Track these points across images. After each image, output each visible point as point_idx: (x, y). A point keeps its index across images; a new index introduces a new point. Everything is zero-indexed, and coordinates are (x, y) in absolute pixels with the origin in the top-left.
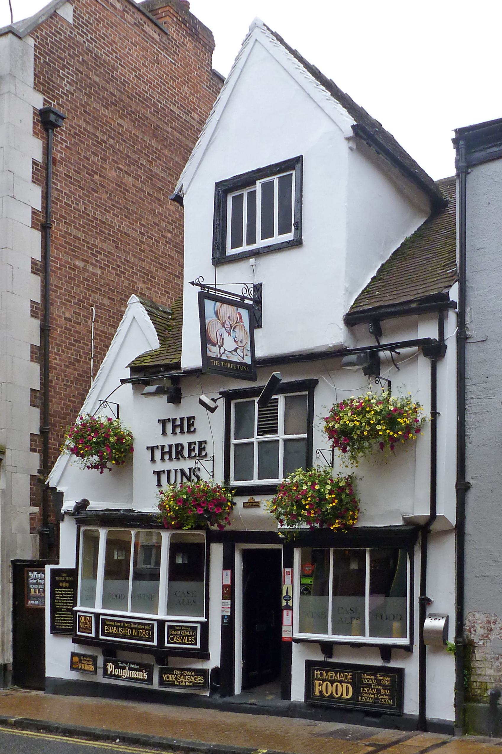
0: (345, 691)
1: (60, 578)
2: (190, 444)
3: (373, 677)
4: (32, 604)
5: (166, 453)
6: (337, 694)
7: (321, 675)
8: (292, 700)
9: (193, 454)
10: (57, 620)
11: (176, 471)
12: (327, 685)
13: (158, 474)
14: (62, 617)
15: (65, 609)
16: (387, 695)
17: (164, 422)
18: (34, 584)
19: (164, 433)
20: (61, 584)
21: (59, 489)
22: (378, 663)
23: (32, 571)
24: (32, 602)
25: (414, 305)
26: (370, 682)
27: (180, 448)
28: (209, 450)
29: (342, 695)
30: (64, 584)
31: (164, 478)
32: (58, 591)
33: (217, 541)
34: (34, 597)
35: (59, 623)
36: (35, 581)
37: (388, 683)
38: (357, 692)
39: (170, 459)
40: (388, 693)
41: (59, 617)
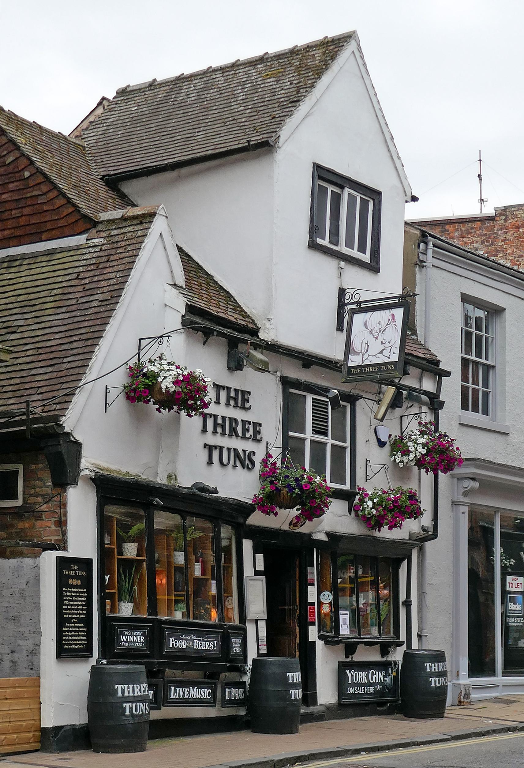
1: (69, 573)
9: (248, 435)
10: (66, 636)
11: (229, 449)
13: (210, 448)
14: (72, 631)
15: (75, 618)
20: (70, 581)
21: (78, 436)
30: (75, 582)
32: (66, 592)
35: (69, 640)
41: (68, 631)
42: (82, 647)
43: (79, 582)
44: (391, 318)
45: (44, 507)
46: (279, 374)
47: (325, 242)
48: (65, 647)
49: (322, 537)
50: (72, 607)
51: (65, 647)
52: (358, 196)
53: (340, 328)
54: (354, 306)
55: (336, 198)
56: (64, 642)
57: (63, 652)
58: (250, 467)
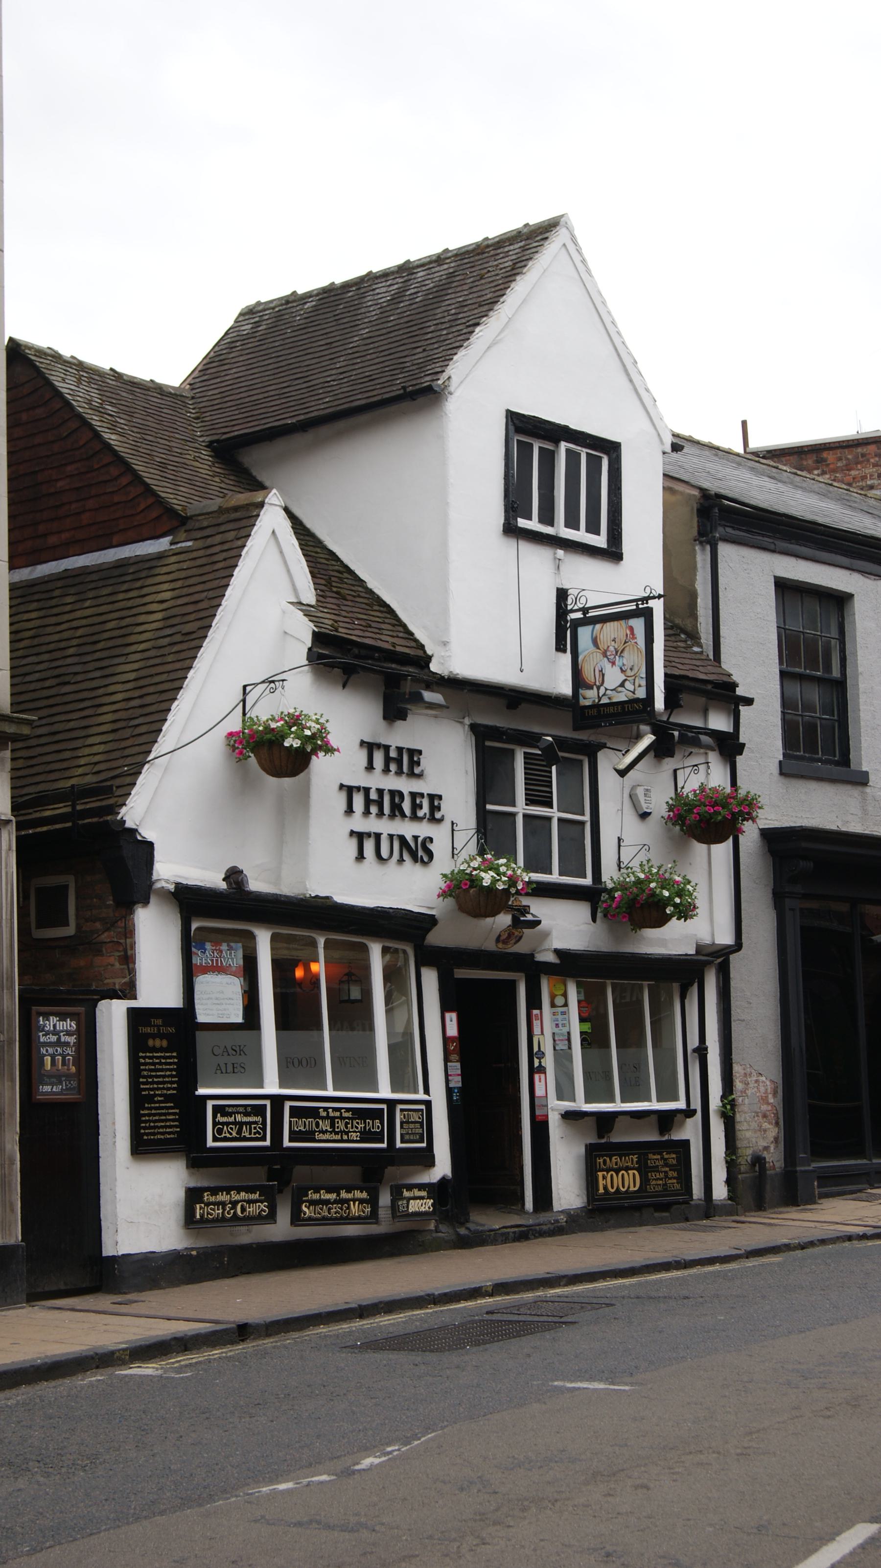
0: (630, 1181)
1: (148, 1030)
2: (414, 795)
3: (659, 1157)
4: (47, 1093)
5: (374, 802)
6: (623, 1187)
7: (605, 1162)
8: (555, 1209)
9: (420, 814)
10: (145, 1122)
11: (391, 836)
12: (612, 1176)
13: (360, 837)
14: (155, 1115)
15: (160, 1095)
16: (674, 1178)
17: (370, 747)
18: (50, 1044)
19: (370, 767)
20: (151, 1043)
22: (653, 1137)
23: (46, 1016)
24: (47, 1088)
25: (709, 687)
26: (657, 1163)
27: (397, 800)
28: (447, 809)
29: (629, 1187)
30: (158, 1043)
31: (369, 847)
32: (144, 1058)
33: (429, 964)
34: (50, 1076)
35: (150, 1128)
36: (53, 1038)
37: (675, 1162)
38: (645, 1181)
39: (381, 814)
40: (675, 1175)
41: (149, 1115)
42: (172, 1136)
43: (165, 1043)
44: (628, 632)
45: (104, 937)
46: (467, 721)
47: (533, 524)
48: (145, 1137)
49: (551, 958)
50: (155, 1080)
51: (145, 1137)
52: (584, 453)
53: (560, 647)
54: (579, 615)
55: (548, 460)
56: (142, 1131)
57: (143, 1146)
58: (426, 859)
